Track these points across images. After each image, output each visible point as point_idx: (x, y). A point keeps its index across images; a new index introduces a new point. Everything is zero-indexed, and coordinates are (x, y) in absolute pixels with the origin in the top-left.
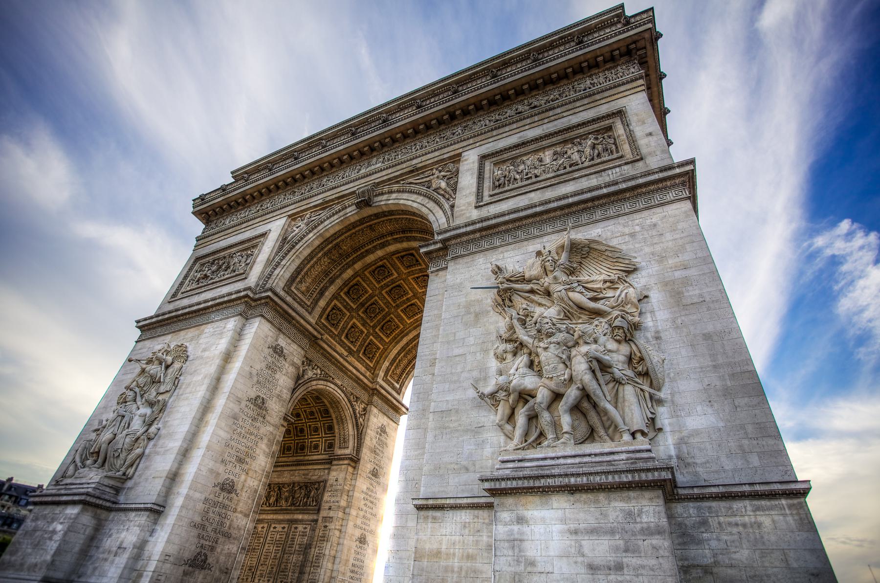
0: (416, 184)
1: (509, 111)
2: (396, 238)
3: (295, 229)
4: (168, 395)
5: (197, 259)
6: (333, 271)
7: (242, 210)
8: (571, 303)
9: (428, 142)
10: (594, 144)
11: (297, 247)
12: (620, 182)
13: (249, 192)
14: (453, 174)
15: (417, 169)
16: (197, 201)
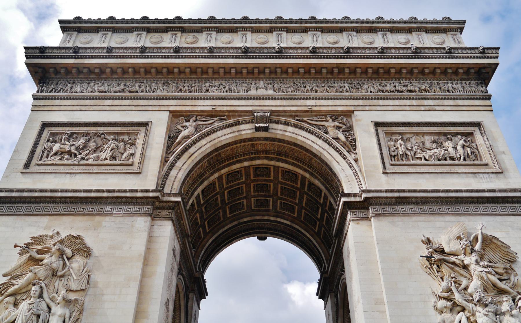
0: (310, 124)
1: (388, 85)
2: (268, 157)
3: (181, 128)
4: (81, 292)
5: (45, 125)
6: (206, 173)
7: (93, 79)
8: (490, 282)
9: (317, 86)
10: (464, 145)
11: (191, 150)
12: (497, 191)
13: (110, 66)
14: (348, 128)
15: (312, 111)
16: (30, 51)
